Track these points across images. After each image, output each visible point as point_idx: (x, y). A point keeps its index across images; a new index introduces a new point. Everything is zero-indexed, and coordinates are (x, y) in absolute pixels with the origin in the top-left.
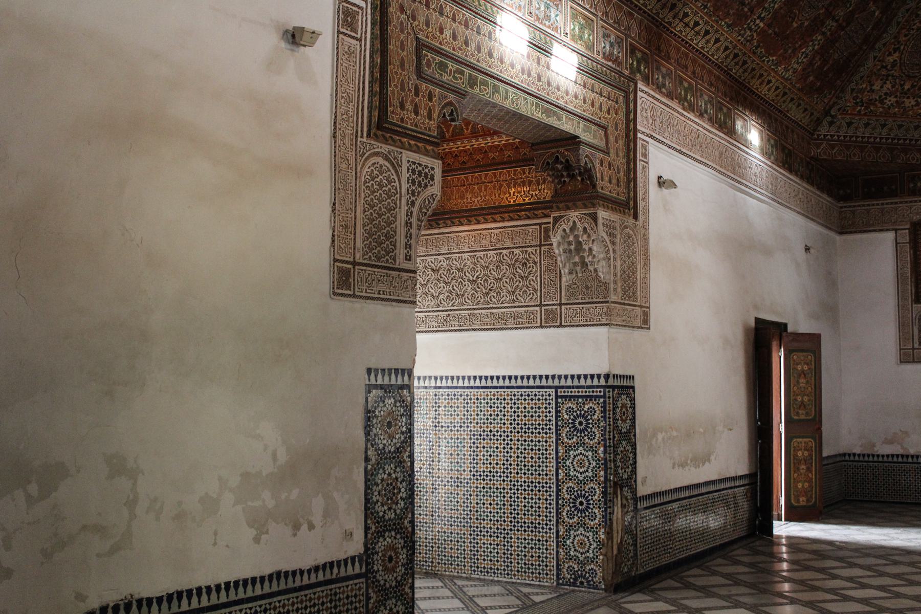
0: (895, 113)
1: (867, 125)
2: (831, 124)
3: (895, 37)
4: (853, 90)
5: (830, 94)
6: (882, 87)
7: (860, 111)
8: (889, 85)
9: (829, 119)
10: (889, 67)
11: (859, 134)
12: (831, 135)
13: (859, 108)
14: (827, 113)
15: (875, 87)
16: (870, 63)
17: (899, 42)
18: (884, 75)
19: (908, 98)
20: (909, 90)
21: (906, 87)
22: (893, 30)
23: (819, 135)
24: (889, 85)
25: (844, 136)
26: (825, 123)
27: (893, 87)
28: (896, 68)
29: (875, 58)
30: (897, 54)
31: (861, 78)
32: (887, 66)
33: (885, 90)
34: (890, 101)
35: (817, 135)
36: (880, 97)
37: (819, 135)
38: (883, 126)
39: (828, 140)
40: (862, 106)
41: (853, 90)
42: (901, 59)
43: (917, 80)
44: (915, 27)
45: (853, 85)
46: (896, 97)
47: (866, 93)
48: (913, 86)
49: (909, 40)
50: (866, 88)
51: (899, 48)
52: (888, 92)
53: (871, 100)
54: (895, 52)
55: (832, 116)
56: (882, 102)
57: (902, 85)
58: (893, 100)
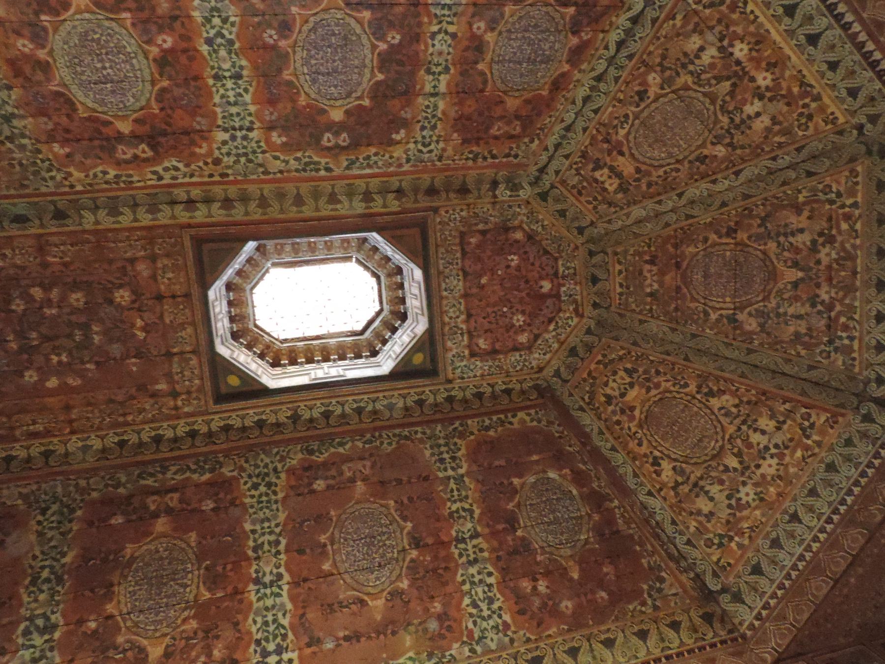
0: (779, 495)
1: (776, 543)
2: (738, 598)
3: (634, 459)
4: (689, 542)
5: (662, 580)
6: (712, 499)
7: (740, 546)
8: (714, 489)
9: (725, 599)
10: (680, 479)
11: (788, 563)
12: (764, 608)
13: (733, 545)
14: (709, 596)
15: (706, 510)
16: (655, 503)
17: (645, 455)
18: (690, 491)
19: (758, 466)
20: (741, 463)
21: (733, 463)
22: (619, 458)
23: (751, 627)
24: (714, 489)
25: (779, 588)
26: (730, 608)
27: (721, 482)
28: (688, 471)
29: (650, 493)
30: (666, 465)
31: (674, 522)
32: (676, 481)
33: (721, 497)
34: (747, 494)
35: (749, 628)
36: (730, 506)
37: (751, 627)
38: (795, 518)
39: (768, 616)
40: (731, 539)
41: (689, 542)
42: (675, 460)
43: (730, 447)
44: (633, 430)
45: (680, 541)
46: (744, 484)
47: (709, 525)
48: (739, 455)
49: (649, 441)
50: (700, 523)
51: (655, 458)
52: (726, 493)
53: (728, 522)
54: (659, 465)
55: (724, 590)
56: (740, 506)
57: (727, 469)
58: (749, 489)
